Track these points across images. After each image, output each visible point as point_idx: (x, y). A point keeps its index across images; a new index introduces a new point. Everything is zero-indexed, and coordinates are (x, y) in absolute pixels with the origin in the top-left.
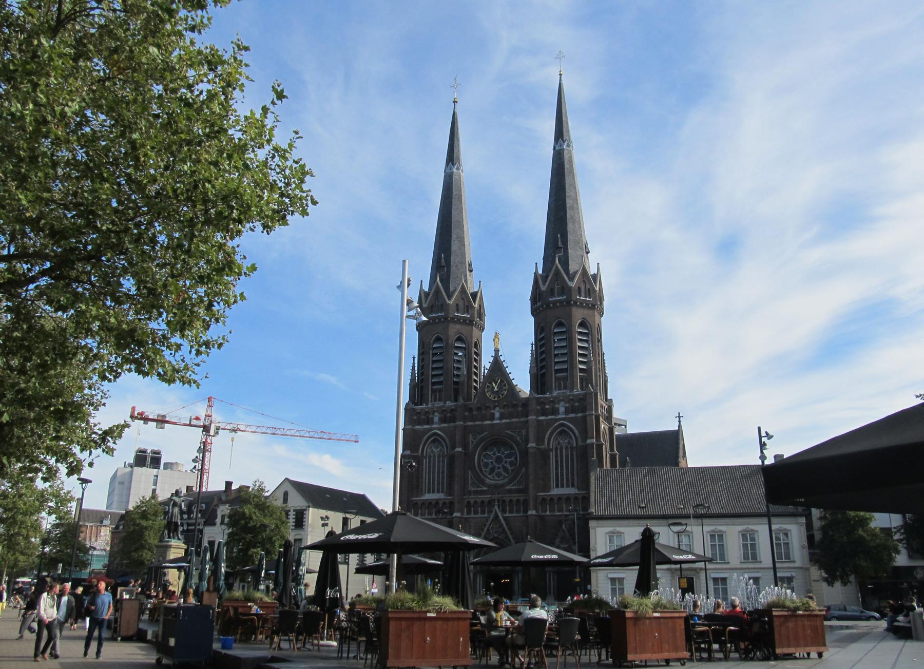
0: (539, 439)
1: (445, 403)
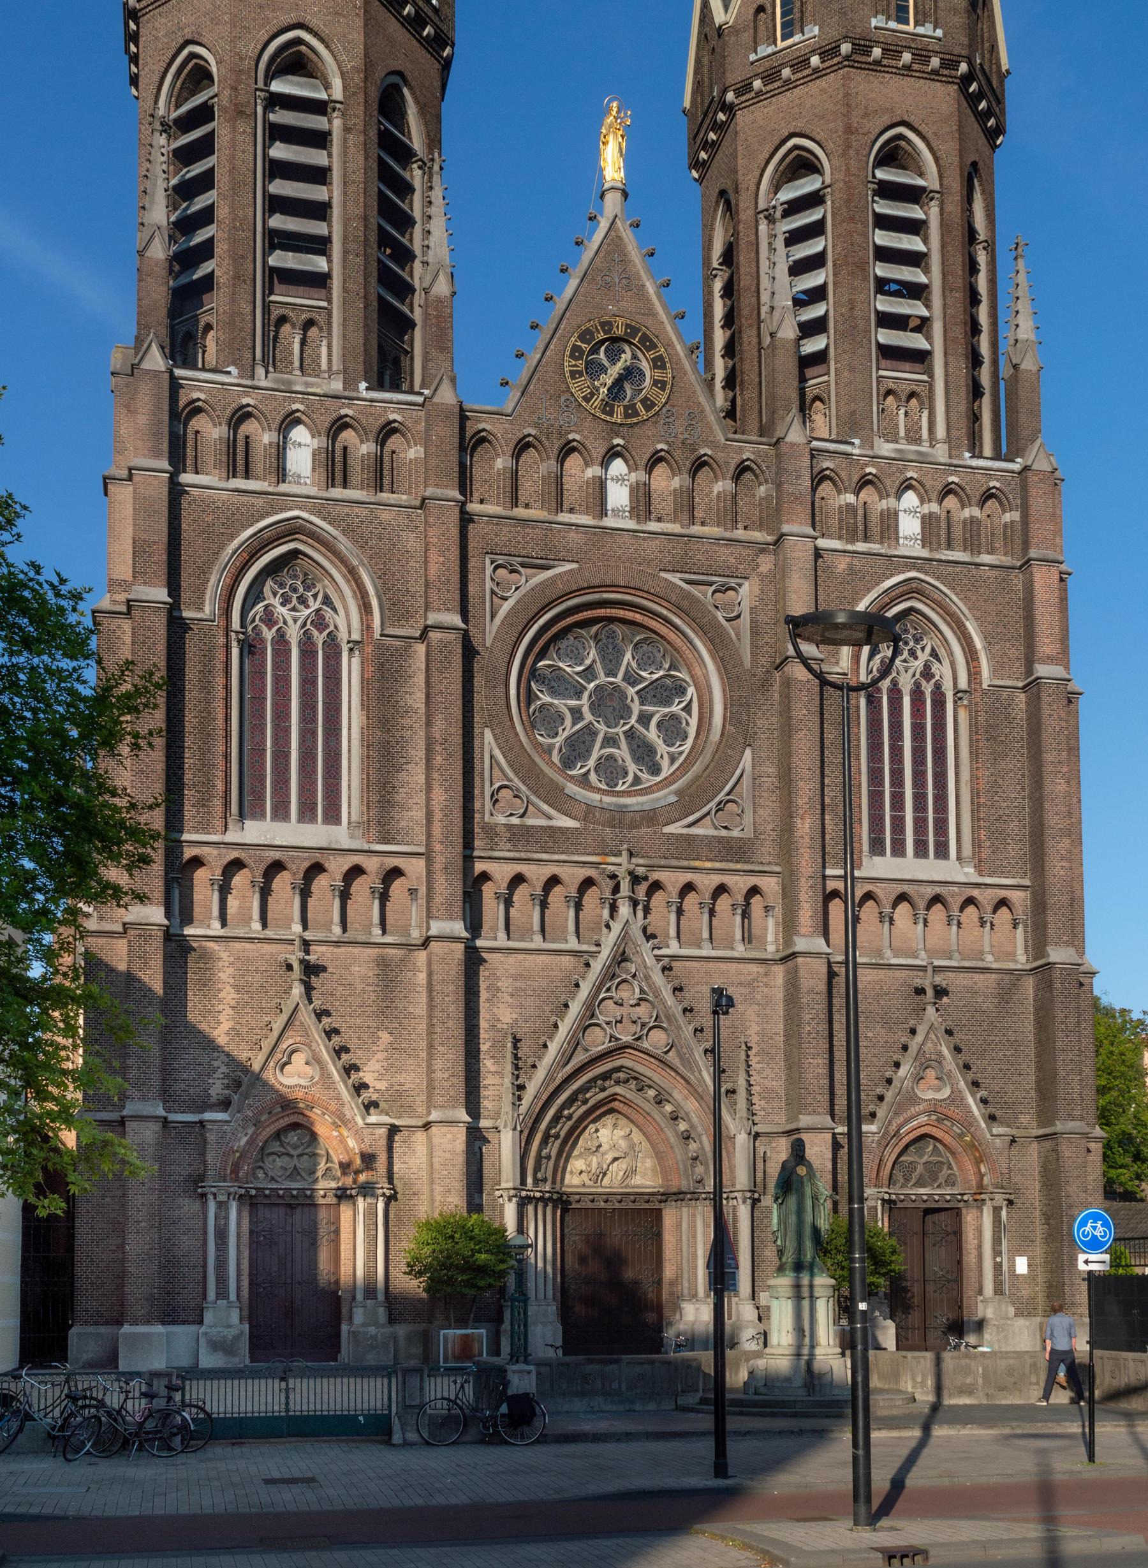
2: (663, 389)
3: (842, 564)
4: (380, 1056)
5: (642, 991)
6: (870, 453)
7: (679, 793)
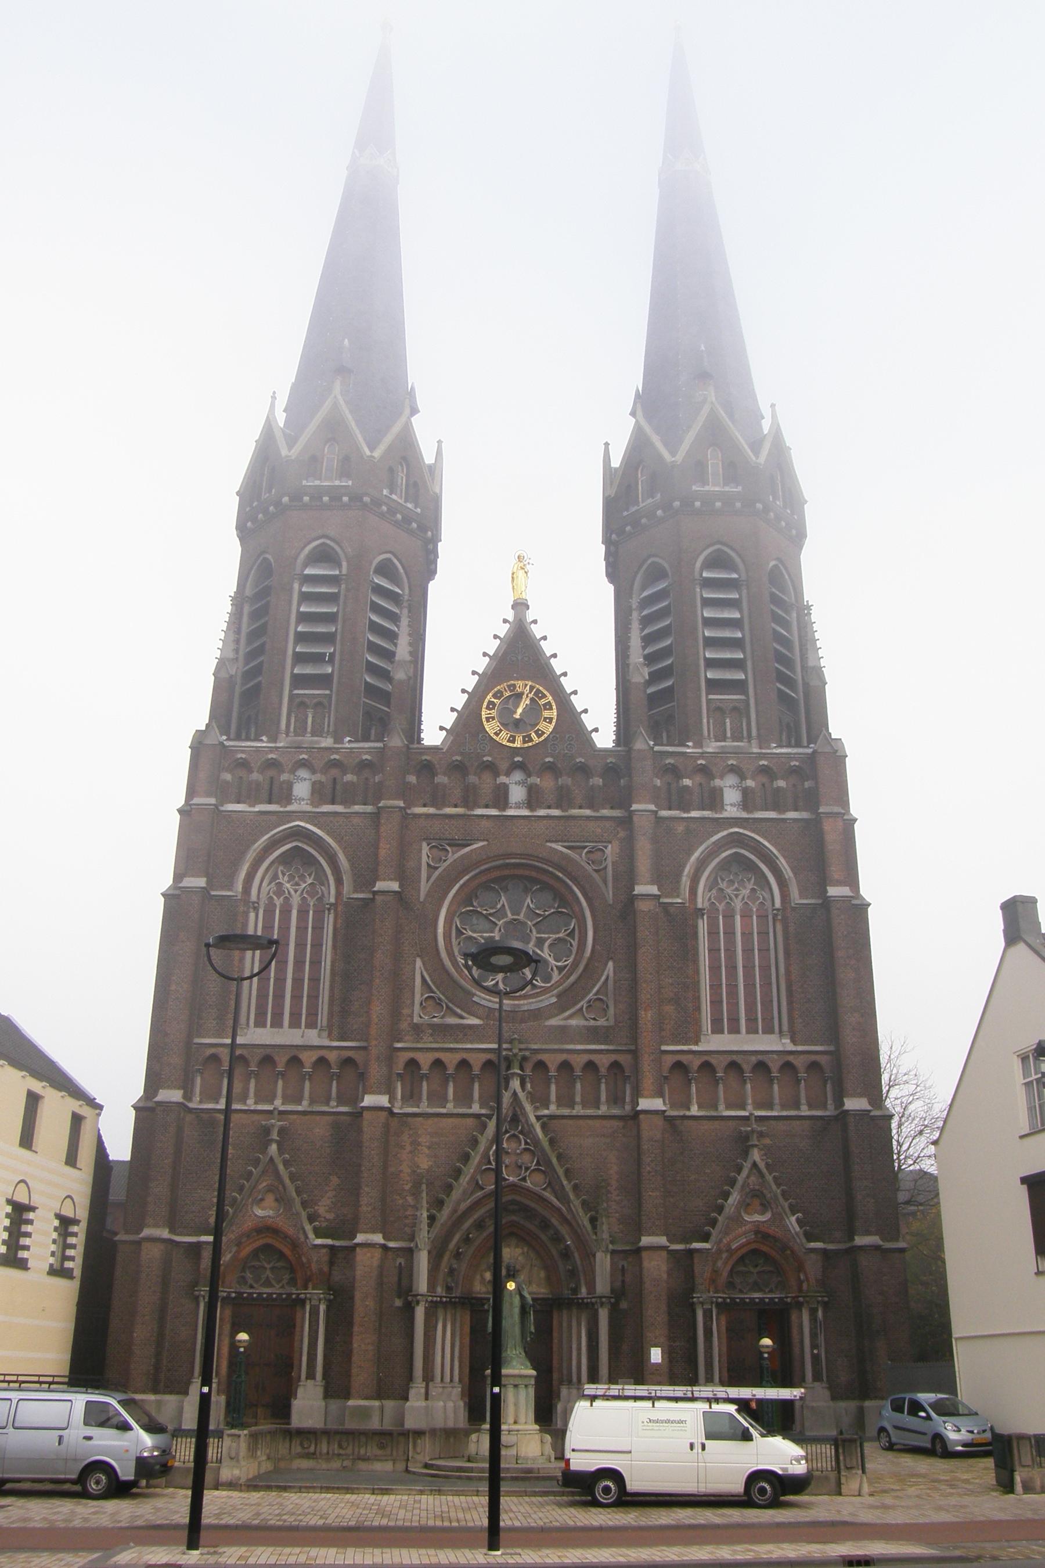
0: (666, 875)
1: (338, 740)
2: (550, 723)
3: (680, 828)
4: (330, 1194)
5: (526, 1143)
6: (700, 751)
7: (559, 996)
